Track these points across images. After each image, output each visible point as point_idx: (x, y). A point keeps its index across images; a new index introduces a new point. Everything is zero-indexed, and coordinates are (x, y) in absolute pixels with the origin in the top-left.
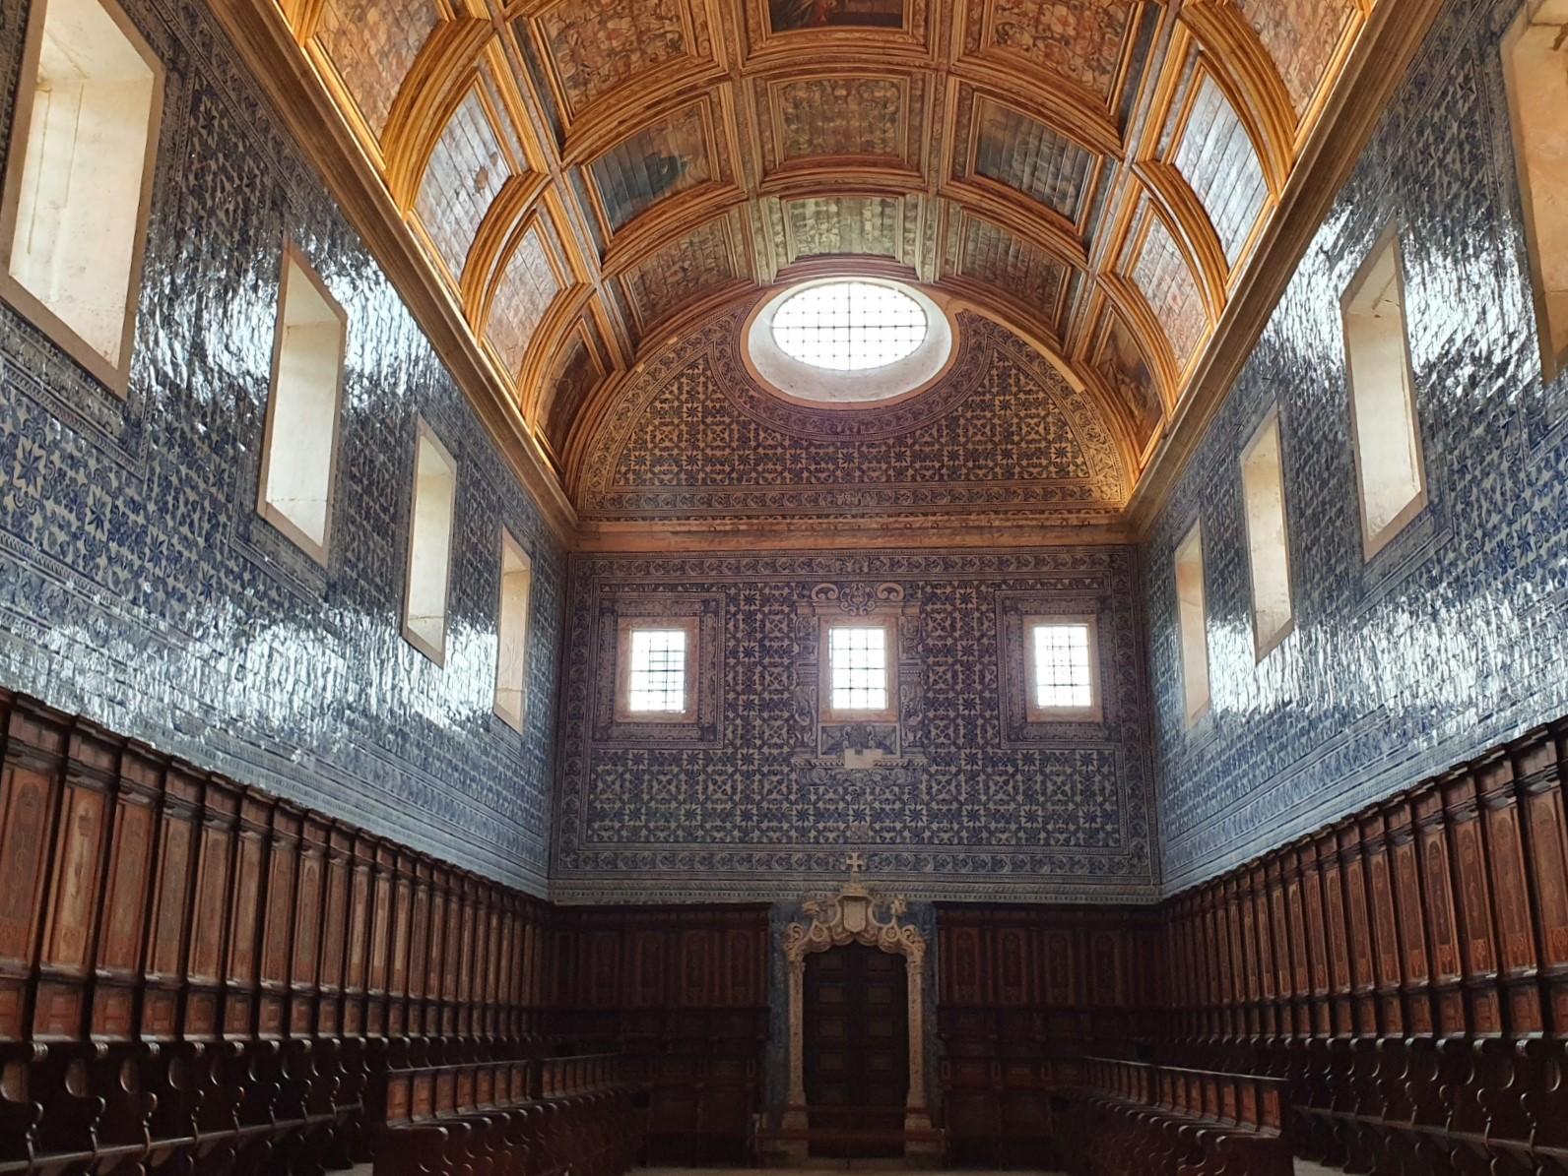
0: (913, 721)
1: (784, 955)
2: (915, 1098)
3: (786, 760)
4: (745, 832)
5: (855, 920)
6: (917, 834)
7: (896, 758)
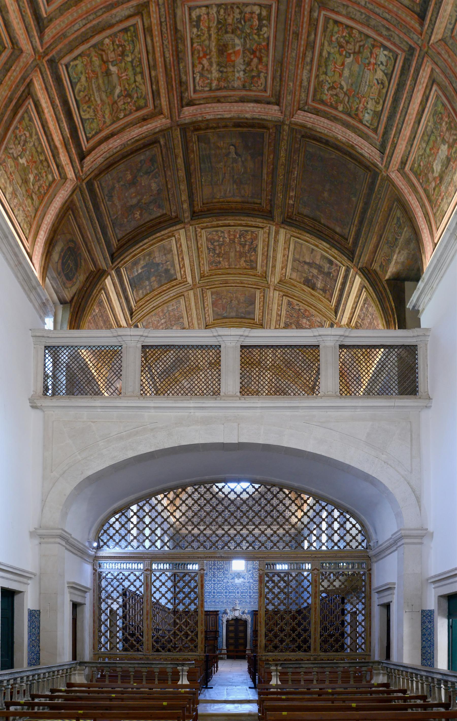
0: (250, 572)
1: (222, 621)
2: (248, 647)
3: (222, 581)
4: (214, 596)
5: (237, 614)
6: (250, 596)
7: (246, 581)
